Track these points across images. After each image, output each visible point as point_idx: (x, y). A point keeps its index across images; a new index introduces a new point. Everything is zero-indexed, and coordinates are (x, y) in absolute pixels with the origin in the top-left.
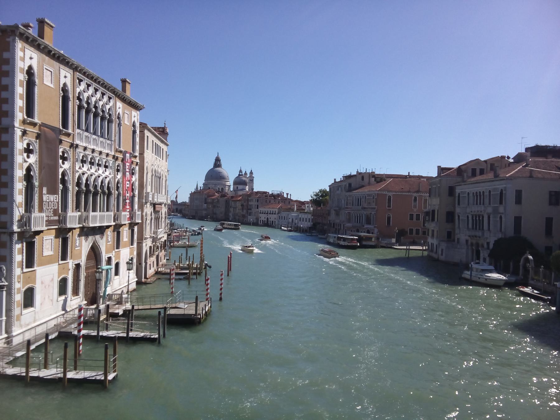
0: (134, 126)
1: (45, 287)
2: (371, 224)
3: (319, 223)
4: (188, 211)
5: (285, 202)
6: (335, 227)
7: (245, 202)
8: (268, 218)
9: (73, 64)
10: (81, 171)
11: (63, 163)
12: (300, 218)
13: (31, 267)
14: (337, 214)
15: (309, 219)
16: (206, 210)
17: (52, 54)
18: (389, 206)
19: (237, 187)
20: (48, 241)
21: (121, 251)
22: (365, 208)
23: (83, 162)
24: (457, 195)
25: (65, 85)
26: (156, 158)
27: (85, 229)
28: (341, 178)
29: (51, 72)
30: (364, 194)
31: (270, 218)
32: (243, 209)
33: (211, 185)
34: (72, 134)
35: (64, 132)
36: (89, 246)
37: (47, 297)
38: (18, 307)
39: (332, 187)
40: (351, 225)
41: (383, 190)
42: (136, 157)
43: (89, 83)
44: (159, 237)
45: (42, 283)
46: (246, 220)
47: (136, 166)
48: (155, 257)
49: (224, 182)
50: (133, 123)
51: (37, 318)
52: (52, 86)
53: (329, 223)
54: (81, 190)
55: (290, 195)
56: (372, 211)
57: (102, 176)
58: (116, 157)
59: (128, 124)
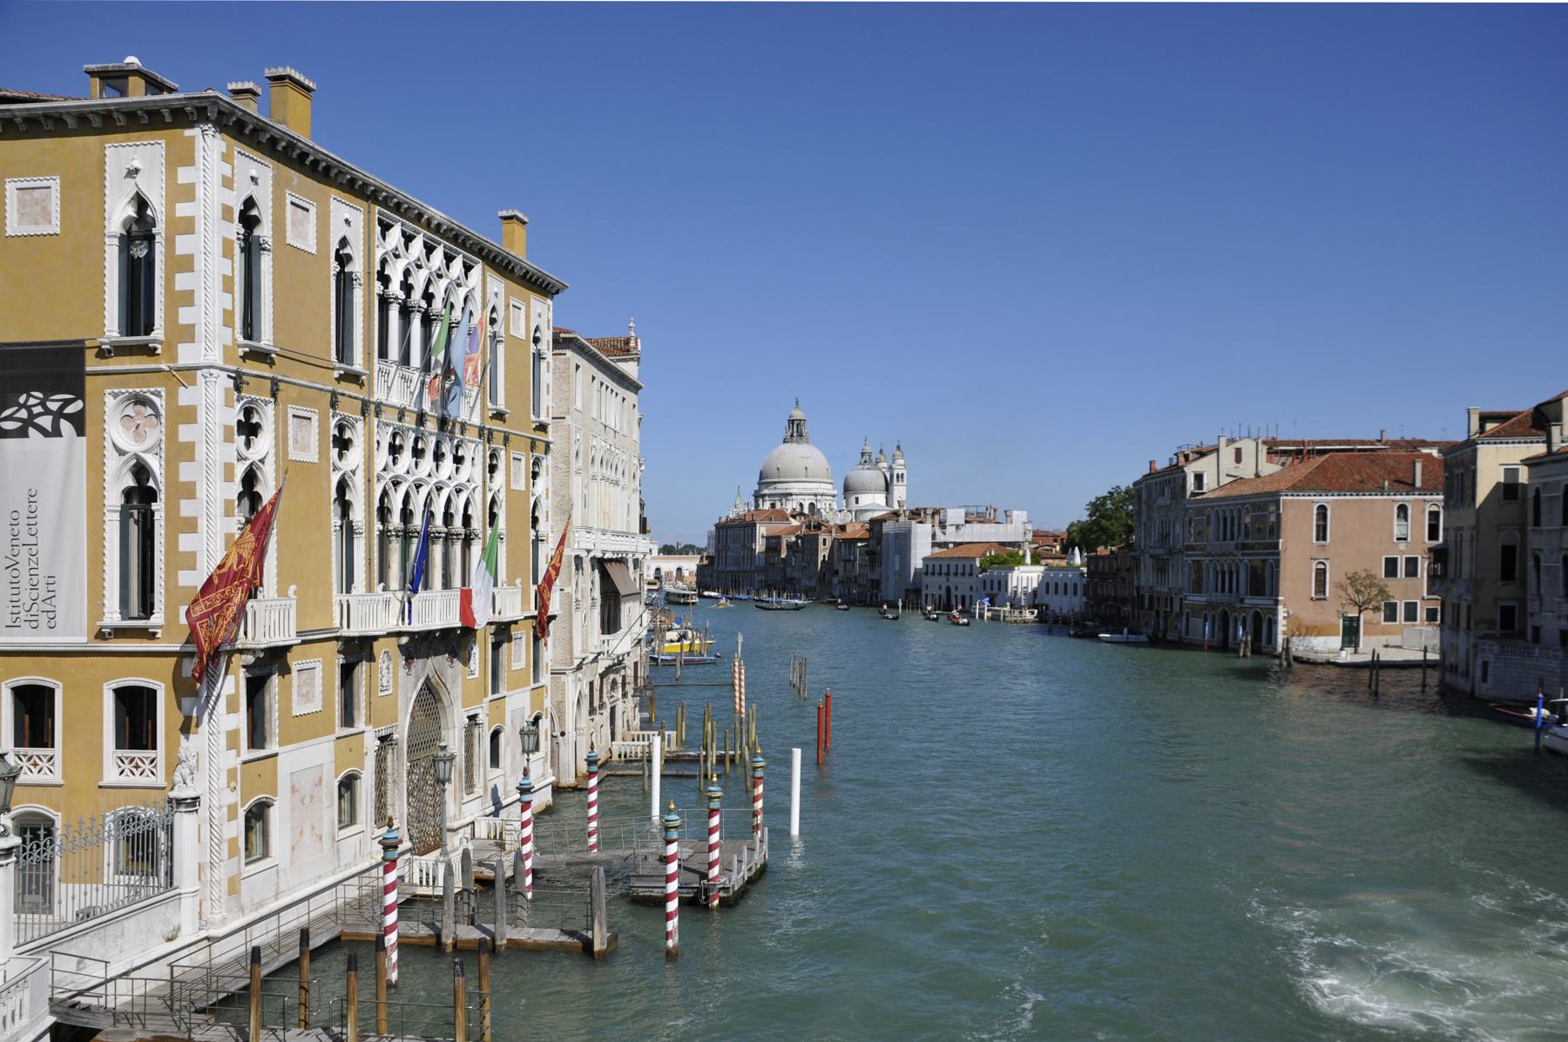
0: (536, 340)
1: (302, 801)
2: (1263, 595)
3: (1106, 600)
4: (712, 576)
6: (1156, 608)
8: (948, 589)
9: (365, 185)
10: (388, 476)
11: (341, 456)
12: (1048, 584)
13: (263, 747)
14: (1161, 567)
15: (1075, 585)
17: (307, 162)
19: (857, 499)
20: (305, 675)
22: (1245, 546)
23: (395, 450)
24: (1531, 495)
28: (1171, 459)
30: (1243, 505)
31: (956, 588)
34: (365, 374)
36: (416, 686)
37: (307, 829)
38: (231, 856)
39: (1143, 485)
40: (1204, 599)
42: (542, 428)
43: (409, 232)
45: (294, 790)
48: (607, 712)
50: (536, 331)
51: (282, 888)
53: (1135, 595)
54: (391, 528)
58: (486, 432)
59: (521, 334)
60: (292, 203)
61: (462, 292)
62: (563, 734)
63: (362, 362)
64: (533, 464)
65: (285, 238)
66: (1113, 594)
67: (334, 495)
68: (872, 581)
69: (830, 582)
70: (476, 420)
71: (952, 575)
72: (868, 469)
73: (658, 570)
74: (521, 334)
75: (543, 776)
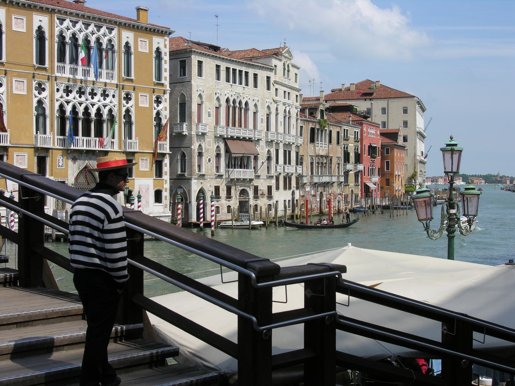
0: (158, 52)
11: (40, 93)
20: (20, 157)
21: (136, 181)
23: (68, 91)
25: (40, 28)
26: (231, 85)
27: (69, 152)
29: (23, 19)
35: (37, 67)
42: (162, 85)
44: (232, 177)
47: (164, 94)
52: (24, 30)
57: (110, 105)
58: (121, 87)
59: (147, 51)
60: (15, 18)
61: (107, 38)
62: (190, 202)
63: (48, 64)
64: (158, 98)
65: (12, 27)
67: (35, 104)
70: (115, 81)
74: (147, 51)
75: (164, 212)
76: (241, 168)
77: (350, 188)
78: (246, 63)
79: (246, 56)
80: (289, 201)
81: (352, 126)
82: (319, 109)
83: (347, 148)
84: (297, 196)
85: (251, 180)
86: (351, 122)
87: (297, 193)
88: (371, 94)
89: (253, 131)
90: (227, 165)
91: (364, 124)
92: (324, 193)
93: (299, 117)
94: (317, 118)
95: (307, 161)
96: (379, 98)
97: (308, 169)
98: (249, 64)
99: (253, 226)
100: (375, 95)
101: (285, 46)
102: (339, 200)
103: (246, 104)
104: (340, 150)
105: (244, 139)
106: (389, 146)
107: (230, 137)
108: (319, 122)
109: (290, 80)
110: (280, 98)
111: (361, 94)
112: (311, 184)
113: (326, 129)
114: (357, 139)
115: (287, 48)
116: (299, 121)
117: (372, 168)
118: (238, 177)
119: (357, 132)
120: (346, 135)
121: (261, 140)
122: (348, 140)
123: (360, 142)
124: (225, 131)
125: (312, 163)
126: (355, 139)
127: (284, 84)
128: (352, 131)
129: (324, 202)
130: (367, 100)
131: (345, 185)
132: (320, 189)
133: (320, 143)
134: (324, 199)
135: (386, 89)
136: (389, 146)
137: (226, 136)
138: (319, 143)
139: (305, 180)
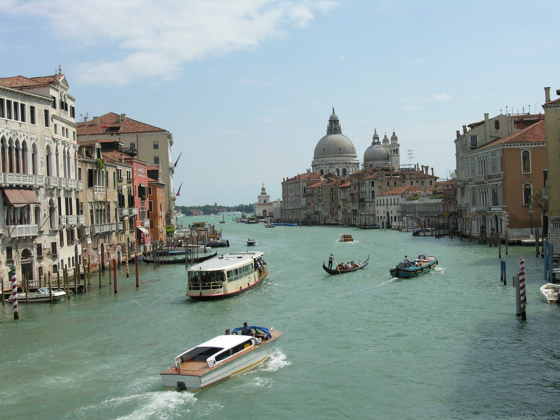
2: (498, 205)
5: (422, 182)
7: (355, 189)
8: (388, 212)
16: (305, 208)
18: (526, 169)
22: (490, 177)
26: (6, 121)
30: (487, 153)
31: (391, 211)
32: (353, 201)
33: (324, 166)
40: (475, 209)
41: (512, 143)
44: (13, 236)
46: (358, 219)
49: (344, 158)
55: (432, 169)
56: (498, 181)
66: (454, 211)
68: (353, 210)
69: (337, 213)
71: (389, 205)
72: (377, 147)
73: (264, 211)
76: (21, 224)
77: (126, 235)
78: (22, 94)
79: (14, 85)
80: (73, 258)
81: (125, 165)
82: (96, 147)
83: (121, 190)
84: (80, 252)
85: (34, 237)
86: (123, 160)
87: (79, 247)
88: (118, 128)
89: (34, 177)
90: (6, 220)
91: (134, 163)
92: (105, 244)
93: (77, 158)
94: (94, 158)
95: (87, 208)
96: (127, 133)
97: (88, 217)
98: (25, 95)
99: (55, 298)
100: (121, 129)
101: (60, 73)
102: (119, 251)
103: (24, 143)
104: (117, 193)
105: (25, 187)
106: (151, 185)
107: (8, 185)
108: (97, 163)
109: (67, 114)
110: (59, 136)
111: (106, 128)
112: (93, 235)
113: (103, 170)
114: (130, 180)
115: (63, 76)
116: (77, 162)
117: (142, 211)
118: (20, 235)
119: (130, 172)
120: (119, 176)
121: (42, 187)
122: (122, 181)
123: (132, 183)
124: (3, 178)
125: (91, 211)
126: (128, 180)
127: (63, 119)
128: (125, 171)
129: (105, 255)
130: (113, 135)
131: (122, 233)
132: (101, 241)
133: (98, 187)
134: (105, 251)
135: (133, 123)
136: (151, 185)
137: (4, 185)
138: (97, 187)
139: (88, 233)
